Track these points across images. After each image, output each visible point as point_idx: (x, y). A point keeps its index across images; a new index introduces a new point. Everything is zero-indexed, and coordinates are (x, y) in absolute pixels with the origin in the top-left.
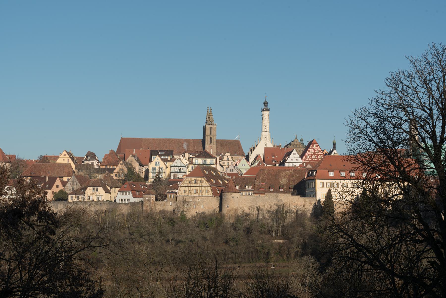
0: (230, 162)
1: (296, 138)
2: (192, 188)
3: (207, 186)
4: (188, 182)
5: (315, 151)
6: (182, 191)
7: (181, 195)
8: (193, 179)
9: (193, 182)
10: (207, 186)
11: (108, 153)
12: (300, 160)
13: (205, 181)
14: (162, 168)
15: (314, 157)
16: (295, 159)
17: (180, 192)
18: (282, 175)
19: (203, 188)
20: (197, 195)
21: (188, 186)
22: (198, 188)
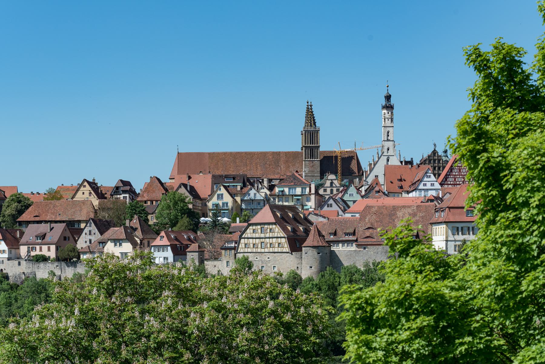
0: (335, 189)
1: (435, 150)
2: (257, 240)
3: (281, 238)
4: (252, 231)
5: (460, 170)
6: (243, 246)
7: (242, 251)
8: (259, 227)
9: (259, 231)
10: (281, 238)
11: (148, 181)
12: (437, 186)
13: (277, 230)
14: (227, 204)
15: (460, 179)
16: (429, 184)
17: (240, 246)
18: (400, 214)
19: (274, 240)
20: (266, 250)
21: (253, 238)
22: (267, 240)
